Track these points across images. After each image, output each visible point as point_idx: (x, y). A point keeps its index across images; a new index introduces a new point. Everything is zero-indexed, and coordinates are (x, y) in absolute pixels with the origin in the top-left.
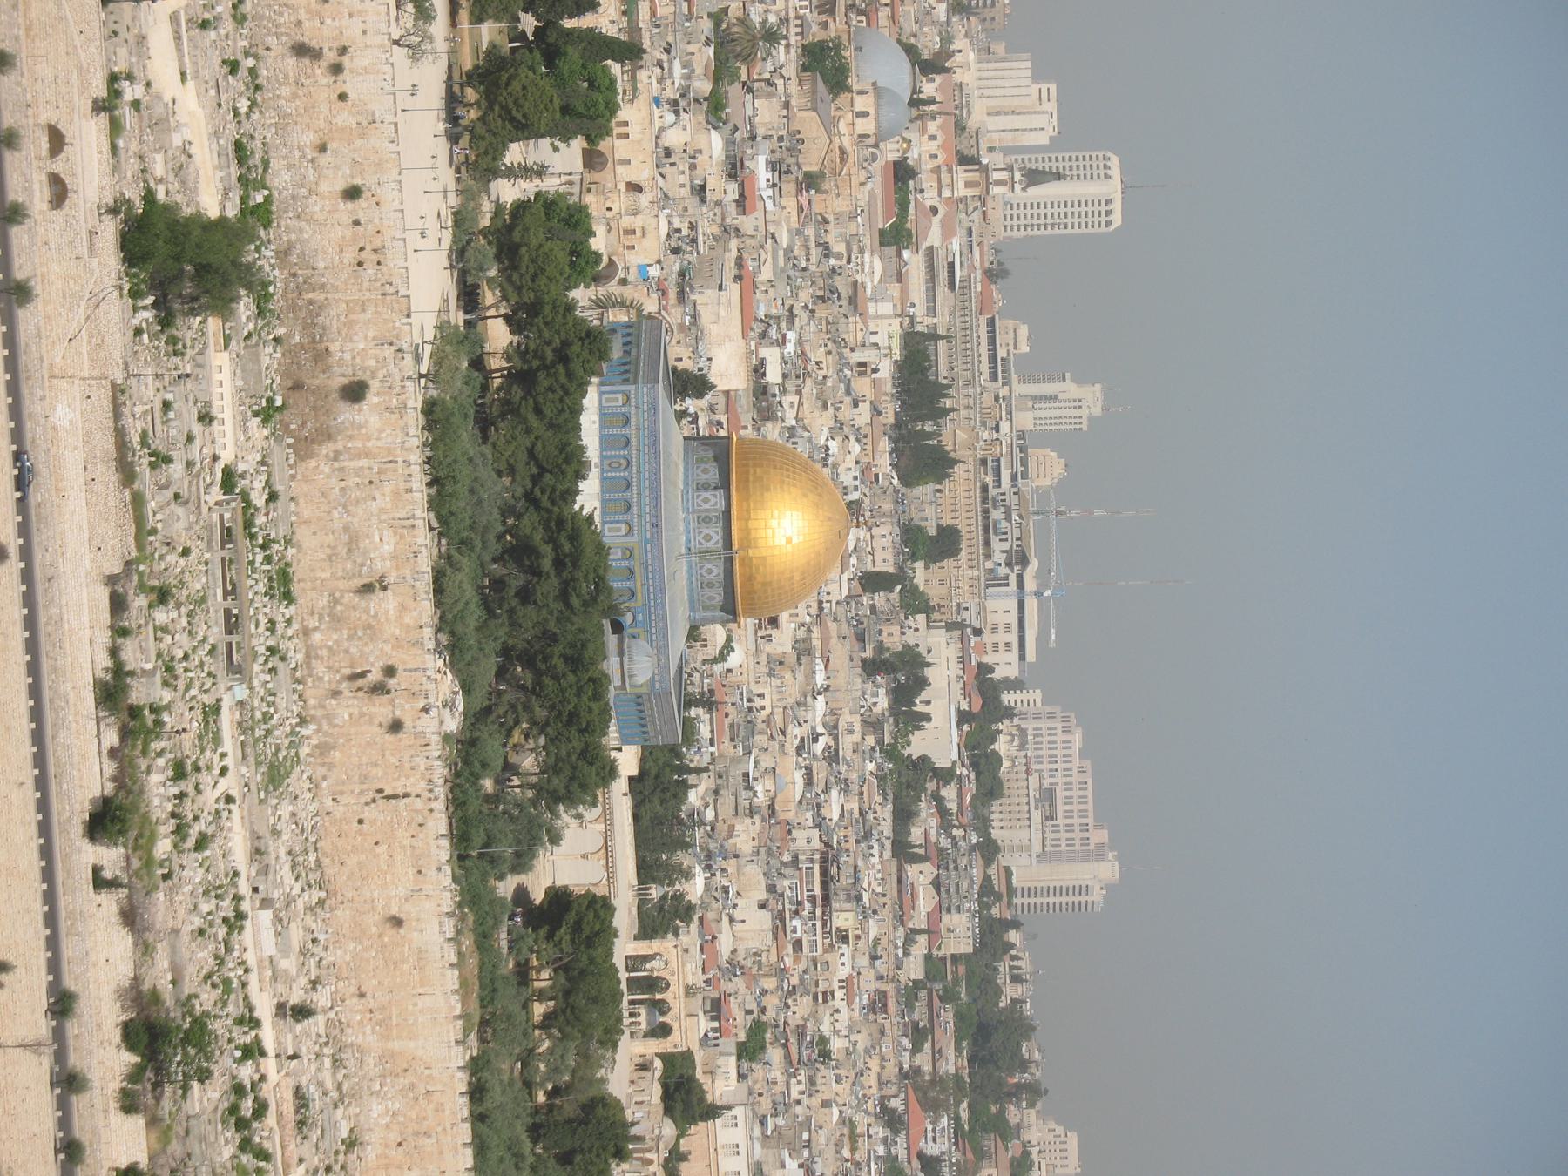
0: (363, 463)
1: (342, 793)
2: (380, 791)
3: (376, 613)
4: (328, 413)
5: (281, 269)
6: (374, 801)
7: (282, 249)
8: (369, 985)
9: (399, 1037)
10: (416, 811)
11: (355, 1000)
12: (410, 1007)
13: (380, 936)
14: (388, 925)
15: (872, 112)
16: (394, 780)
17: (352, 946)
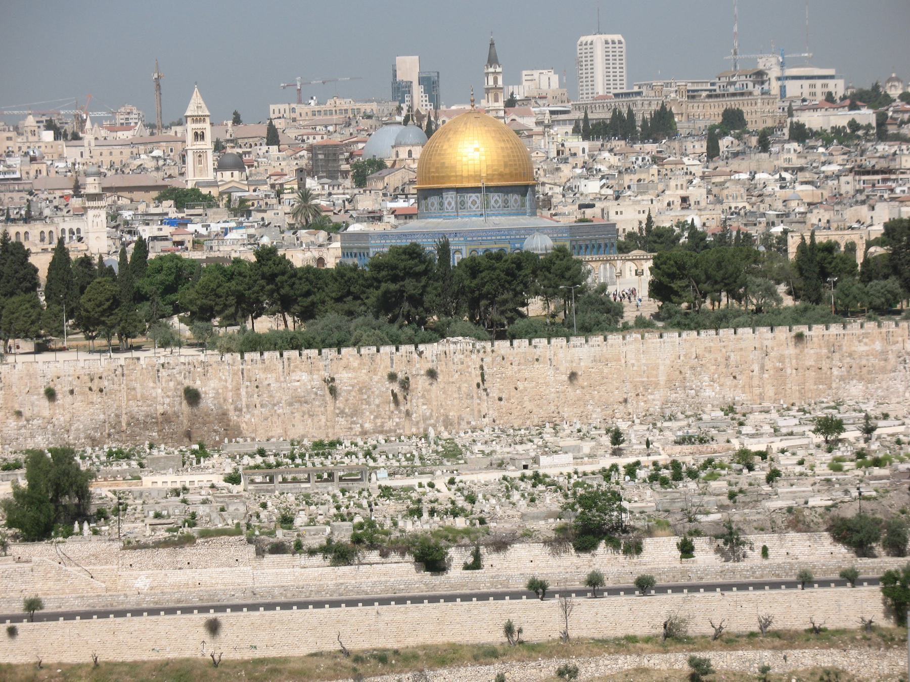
0: (243, 392)
1: (479, 411)
2: (478, 386)
3: (350, 385)
4: (207, 415)
5: (105, 443)
6: (485, 390)
7: (90, 443)
8: (618, 396)
9: (657, 376)
10: (493, 361)
11: (629, 405)
12: (635, 368)
13: (583, 388)
14: (575, 382)
15: (408, 148)
16: (470, 376)
17: (590, 407)
